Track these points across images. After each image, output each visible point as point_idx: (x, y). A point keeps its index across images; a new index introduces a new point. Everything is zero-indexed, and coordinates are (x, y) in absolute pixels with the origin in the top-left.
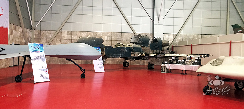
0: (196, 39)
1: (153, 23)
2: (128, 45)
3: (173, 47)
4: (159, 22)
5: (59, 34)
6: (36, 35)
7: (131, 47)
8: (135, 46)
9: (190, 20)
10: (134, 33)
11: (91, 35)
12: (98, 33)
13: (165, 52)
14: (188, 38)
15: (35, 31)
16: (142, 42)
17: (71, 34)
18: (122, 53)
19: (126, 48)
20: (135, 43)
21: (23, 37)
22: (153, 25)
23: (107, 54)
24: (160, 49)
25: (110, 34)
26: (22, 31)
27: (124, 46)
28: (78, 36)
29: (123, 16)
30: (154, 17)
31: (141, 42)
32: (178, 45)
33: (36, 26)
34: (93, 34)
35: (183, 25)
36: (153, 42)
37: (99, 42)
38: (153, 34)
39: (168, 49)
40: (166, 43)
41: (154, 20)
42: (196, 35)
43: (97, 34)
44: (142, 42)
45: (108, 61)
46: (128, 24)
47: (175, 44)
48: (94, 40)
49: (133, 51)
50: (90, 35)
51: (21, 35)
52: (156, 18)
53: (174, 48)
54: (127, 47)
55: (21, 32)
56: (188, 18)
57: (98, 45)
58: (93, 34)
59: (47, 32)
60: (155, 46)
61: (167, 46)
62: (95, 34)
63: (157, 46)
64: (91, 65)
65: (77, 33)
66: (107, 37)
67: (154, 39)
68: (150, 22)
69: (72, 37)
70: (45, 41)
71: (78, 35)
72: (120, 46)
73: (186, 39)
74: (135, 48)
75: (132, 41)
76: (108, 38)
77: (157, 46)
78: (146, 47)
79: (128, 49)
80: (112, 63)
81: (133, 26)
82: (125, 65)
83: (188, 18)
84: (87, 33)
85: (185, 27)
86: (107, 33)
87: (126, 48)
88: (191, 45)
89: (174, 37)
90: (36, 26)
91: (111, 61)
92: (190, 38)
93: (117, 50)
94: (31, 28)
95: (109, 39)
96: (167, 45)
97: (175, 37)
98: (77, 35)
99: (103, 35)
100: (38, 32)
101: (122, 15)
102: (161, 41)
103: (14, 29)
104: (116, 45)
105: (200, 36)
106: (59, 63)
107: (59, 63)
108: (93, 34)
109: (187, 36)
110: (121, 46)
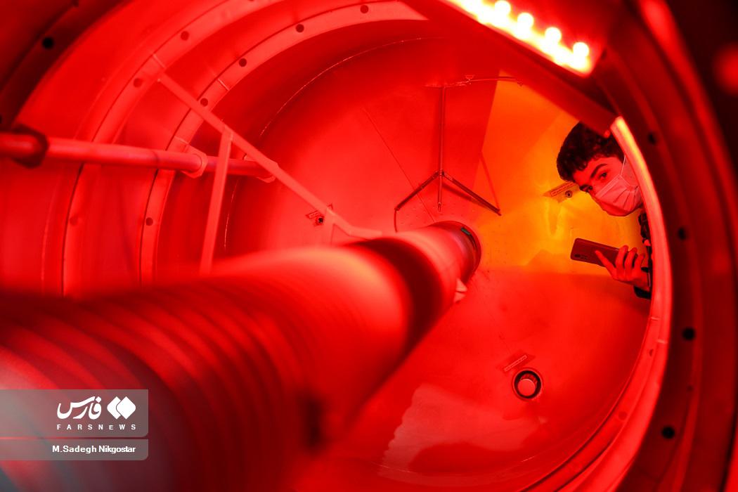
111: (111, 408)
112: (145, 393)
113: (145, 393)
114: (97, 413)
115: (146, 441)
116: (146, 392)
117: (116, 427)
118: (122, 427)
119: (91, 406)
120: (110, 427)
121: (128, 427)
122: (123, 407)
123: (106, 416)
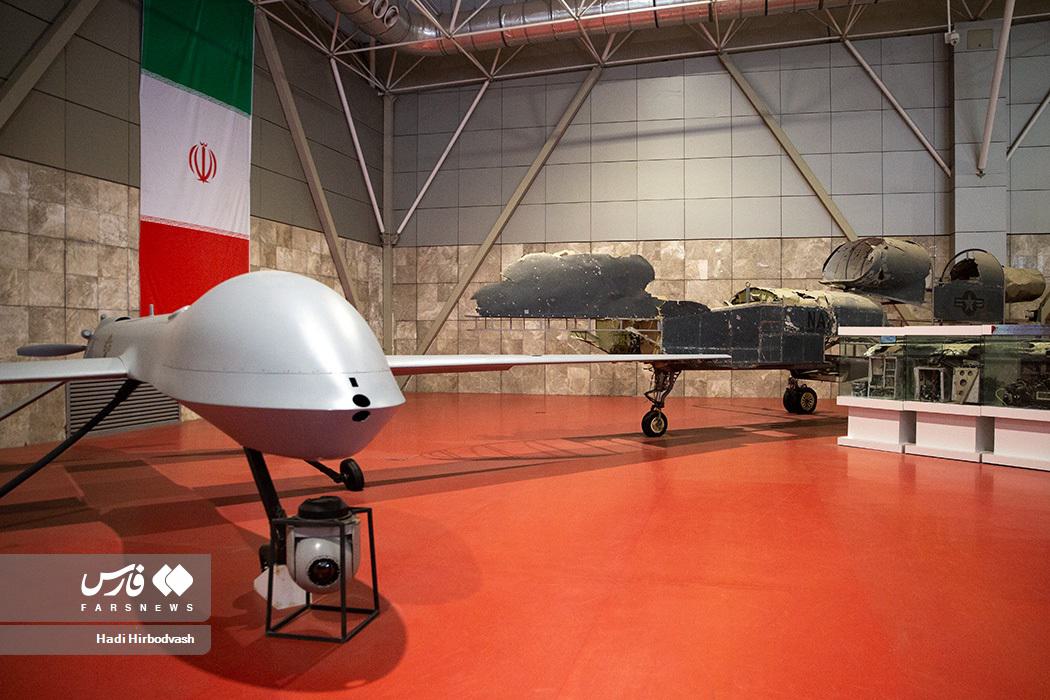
4: (981, 174)
5: (492, 259)
6: (398, 269)
7: (823, 304)
10: (846, 236)
15: (394, 250)
16: (887, 277)
19: (789, 314)
20: (847, 287)
21: (336, 275)
26: (326, 251)
27: (777, 304)
29: (785, 158)
31: (881, 276)
33: (399, 231)
36: (953, 278)
38: (950, 234)
41: (951, 166)
43: (662, 252)
44: (887, 277)
45: (714, 382)
46: (817, 195)
48: (597, 271)
51: (324, 267)
52: (962, 154)
55: (322, 257)
57: (621, 296)
59: (443, 253)
60: (965, 297)
64: (636, 399)
66: (711, 265)
67: (958, 260)
68: (932, 179)
70: (435, 292)
75: (831, 275)
76: (716, 270)
78: (910, 307)
79: (807, 316)
80: (736, 389)
82: (796, 401)
86: (710, 242)
90: (399, 231)
91: (728, 382)
93: (736, 323)
94: (378, 240)
99: (690, 255)
100: (407, 257)
101: (783, 153)
103: (281, 240)
104: (737, 297)
106: (494, 389)
107: (492, 391)
111: (158, 580)
112: (205, 560)
113: (205, 560)
114: (138, 587)
115: (209, 628)
116: (209, 556)
117: (166, 608)
118: (174, 607)
119: (128, 579)
120: (157, 607)
121: (182, 608)
122: (175, 580)
123: (150, 591)
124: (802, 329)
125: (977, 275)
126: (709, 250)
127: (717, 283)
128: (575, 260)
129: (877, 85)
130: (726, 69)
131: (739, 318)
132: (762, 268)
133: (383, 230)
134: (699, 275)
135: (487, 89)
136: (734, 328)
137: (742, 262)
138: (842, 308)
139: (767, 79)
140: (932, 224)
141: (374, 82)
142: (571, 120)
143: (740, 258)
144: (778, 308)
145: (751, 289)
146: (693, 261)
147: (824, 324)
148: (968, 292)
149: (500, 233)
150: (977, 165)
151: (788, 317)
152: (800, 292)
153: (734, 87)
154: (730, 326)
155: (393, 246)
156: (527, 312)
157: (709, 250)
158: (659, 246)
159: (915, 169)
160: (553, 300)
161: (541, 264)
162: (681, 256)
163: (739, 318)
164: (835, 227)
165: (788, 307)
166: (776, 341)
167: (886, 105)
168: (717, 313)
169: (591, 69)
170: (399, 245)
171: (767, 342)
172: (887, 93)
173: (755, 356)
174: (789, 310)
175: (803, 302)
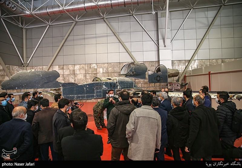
0: (215, 64)
1: (158, 47)
2: (110, 79)
3: (185, 77)
4: (165, 46)
7: (115, 81)
8: (123, 80)
9: (205, 42)
11: (84, 68)
12: (92, 65)
13: (173, 85)
14: (205, 64)
16: (135, 73)
17: (63, 69)
18: (97, 91)
19: (104, 84)
20: (126, 76)
22: (158, 51)
23: (67, 97)
24: (166, 81)
25: (106, 65)
28: (70, 70)
30: (158, 41)
31: (133, 73)
32: (191, 75)
34: (87, 67)
35: (197, 48)
37: (49, 77)
39: (178, 81)
40: (173, 72)
41: (159, 45)
42: (214, 60)
43: (91, 67)
44: (135, 73)
47: (188, 73)
49: (118, 88)
50: (83, 68)
52: (161, 41)
53: (187, 78)
54: (106, 83)
56: (202, 39)
57: (48, 82)
58: (86, 66)
60: (157, 77)
61: (177, 76)
62: (89, 67)
63: (159, 77)
65: (69, 67)
66: (103, 69)
68: (154, 47)
69: (64, 71)
71: (70, 69)
72: (97, 81)
73: (202, 65)
74: (121, 83)
75: (122, 72)
77: (159, 77)
79: (109, 85)
81: (133, 54)
83: (202, 39)
84: (80, 66)
85: (200, 51)
86: (103, 64)
87: (104, 84)
88: (209, 74)
89: (187, 64)
92: (207, 64)
93: (87, 88)
95: (105, 71)
96: (176, 74)
97: (188, 64)
98: (69, 69)
102: (166, 70)
105: (220, 61)
108: (86, 66)
109: (203, 61)
110: (97, 82)
124: (108, 88)
125: (160, 71)
126: (103, 66)
127: (104, 74)
128: (33, 72)
129: (141, 26)
130: (105, 22)
131: (88, 86)
132: (115, 70)
133: (23, 63)
134: (100, 72)
135: (48, 28)
136: (86, 89)
137: (111, 69)
138: (121, 82)
139: (115, 25)
140: (155, 59)
141: (20, 26)
142: (69, 34)
143: (110, 67)
144: (101, 83)
145: (96, 78)
146: (99, 69)
147: (115, 86)
148: (158, 76)
149: (52, 63)
150: (164, 44)
151: (104, 85)
152: (109, 78)
153: (108, 28)
154: (85, 89)
155: (27, 66)
156: (17, 88)
157: (103, 66)
158: (91, 65)
159: (151, 45)
160: (25, 84)
161: (25, 73)
162: (96, 67)
163: (88, 86)
164: (132, 60)
165: (103, 83)
166: (100, 92)
167: (143, 30)
168: (81, 85)
169: (73, 22)
170: (28, 66)
171: (97, 92)
172: (144, 27)
173: (94, 96)
174: (104, 83)
175: (109, 81)
